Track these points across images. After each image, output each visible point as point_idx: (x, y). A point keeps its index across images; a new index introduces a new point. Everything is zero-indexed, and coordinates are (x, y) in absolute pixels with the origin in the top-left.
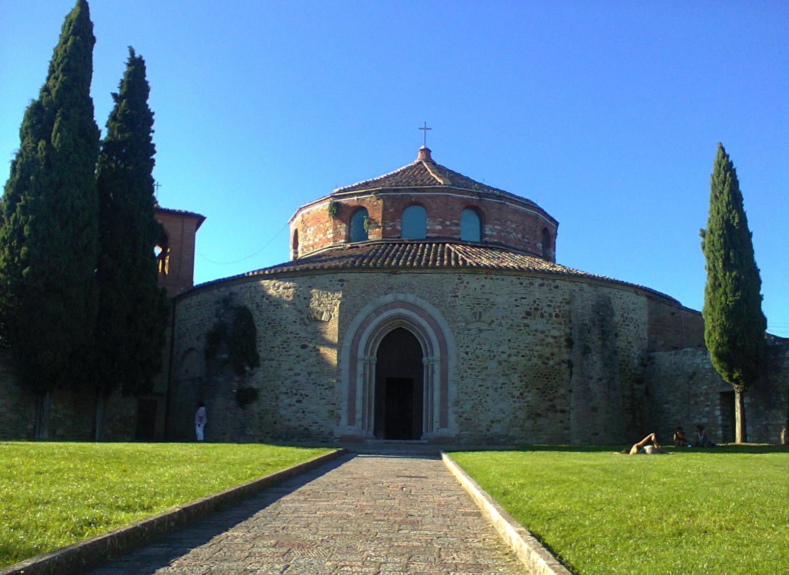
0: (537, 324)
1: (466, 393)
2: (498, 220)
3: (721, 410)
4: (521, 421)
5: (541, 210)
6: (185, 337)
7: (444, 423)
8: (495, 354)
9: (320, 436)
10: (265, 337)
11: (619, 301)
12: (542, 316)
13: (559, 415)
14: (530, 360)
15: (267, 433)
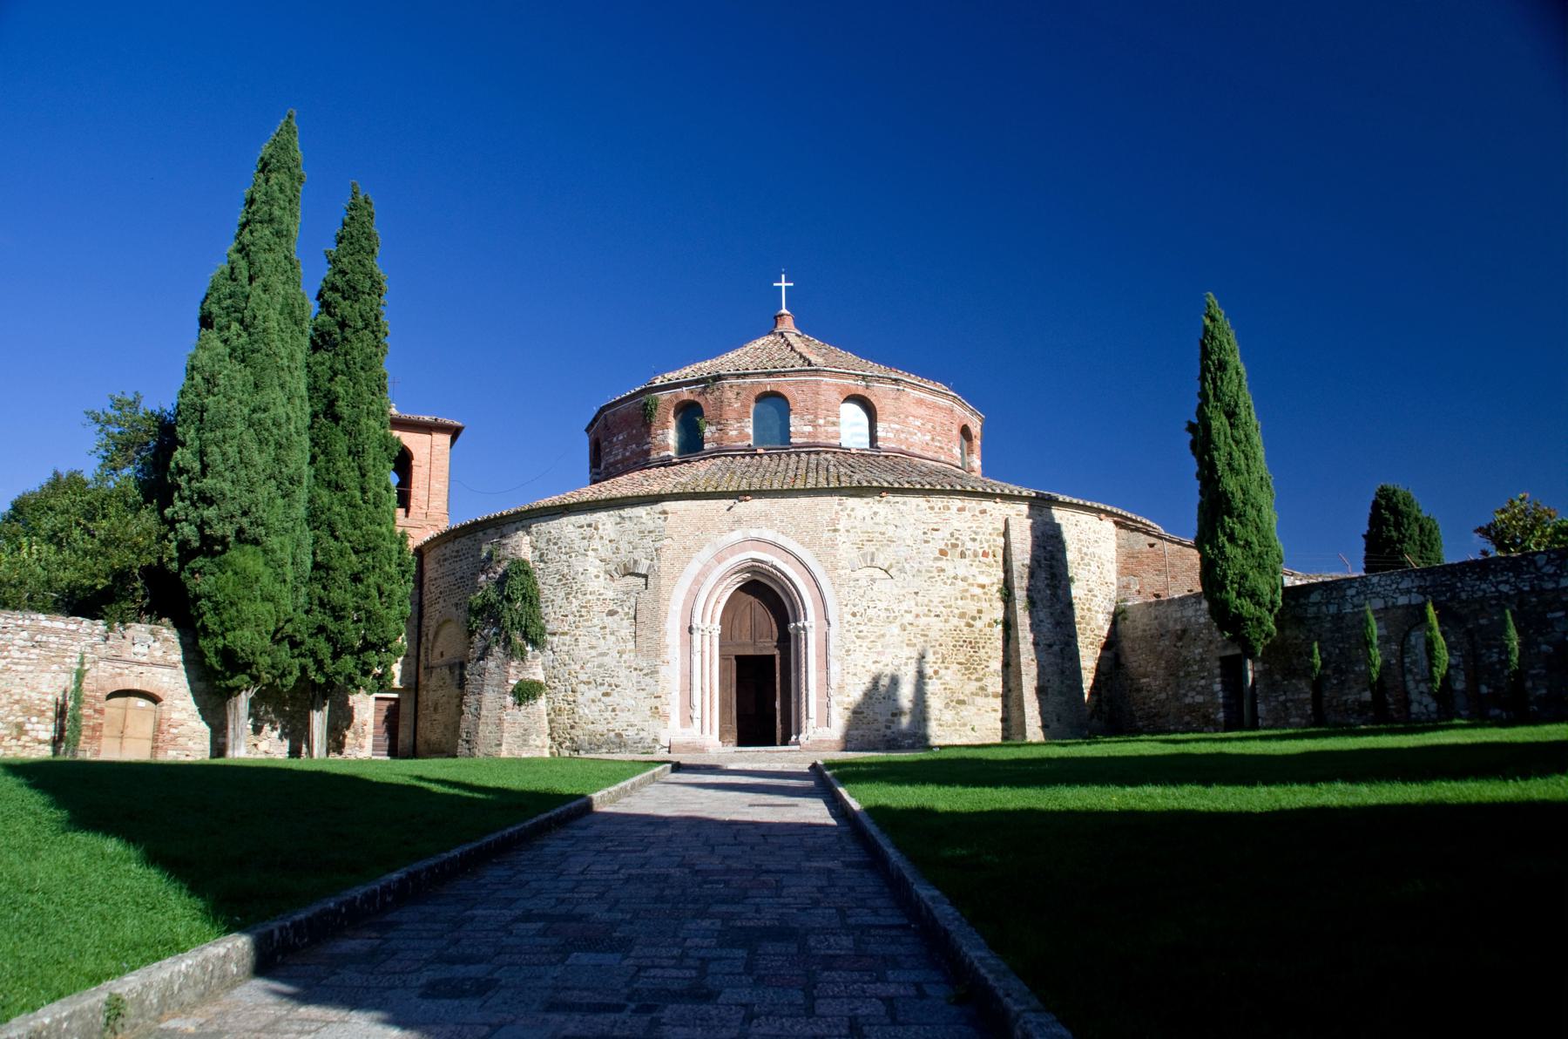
1: (855, 674)
2: (895, 415)
3: (1223, 682)
8: (897, 614)
9: (640, 745)
10: (553, 600)
12: (963, 555)
14: (946, 621)
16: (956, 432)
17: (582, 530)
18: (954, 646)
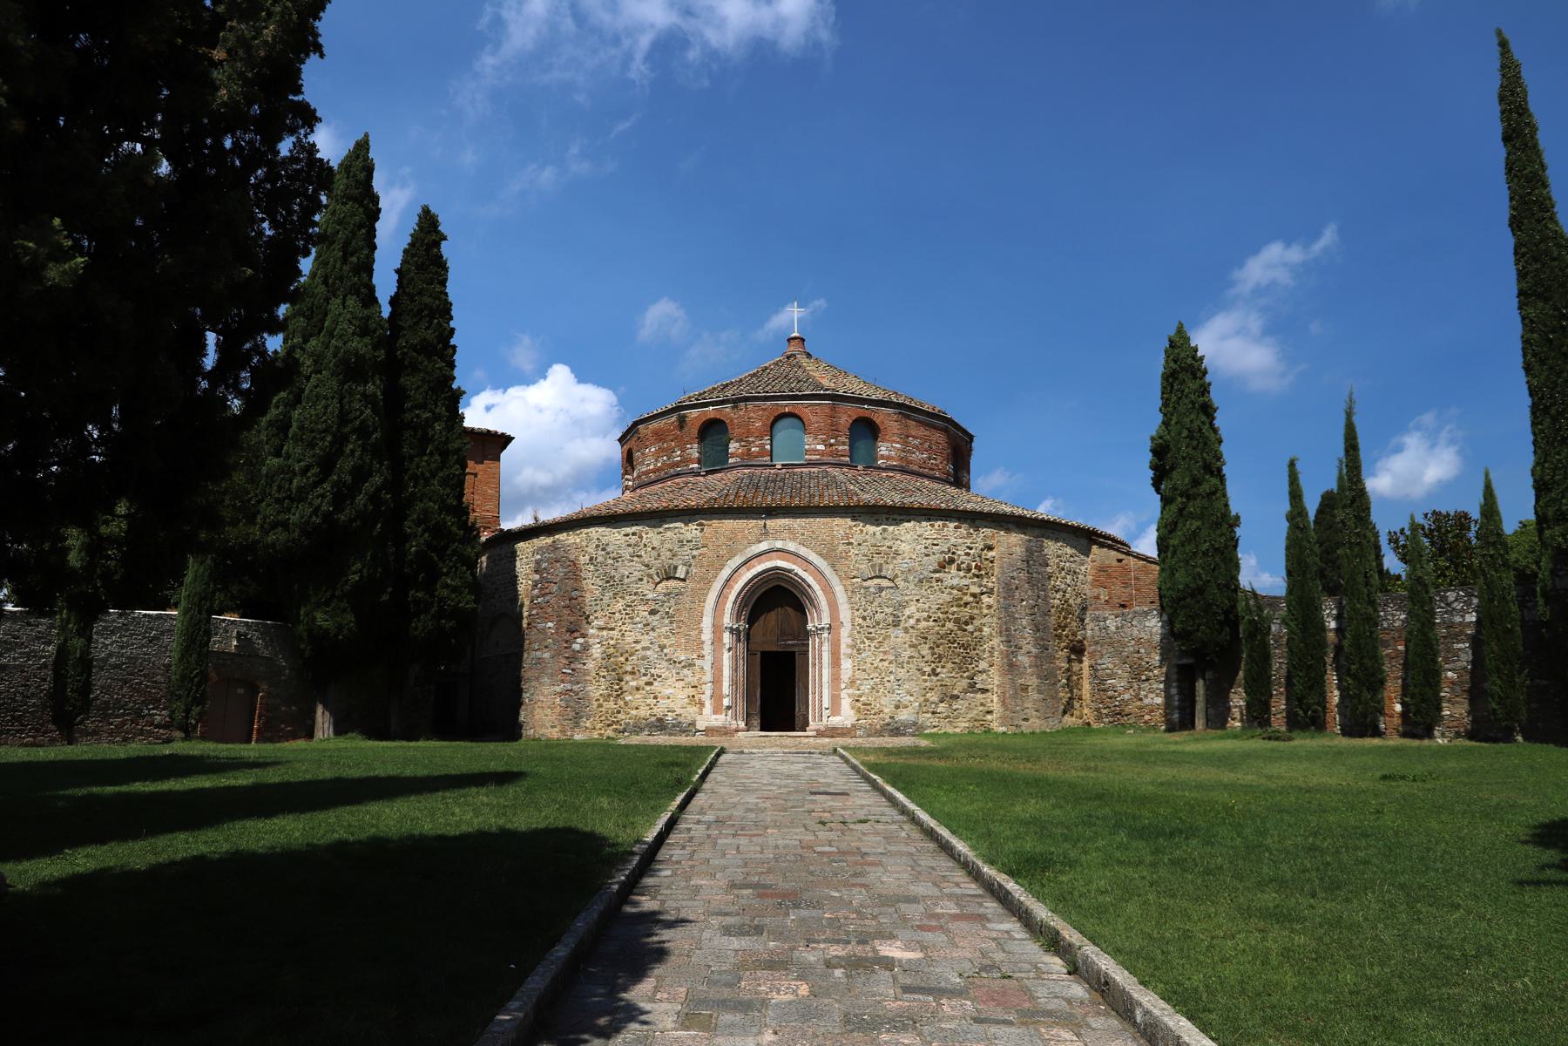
0: (953, 577)
1: (864, 670)
7: (835, 708)
13: (979, 696)
15: (609, 725)
18: (950, 648)
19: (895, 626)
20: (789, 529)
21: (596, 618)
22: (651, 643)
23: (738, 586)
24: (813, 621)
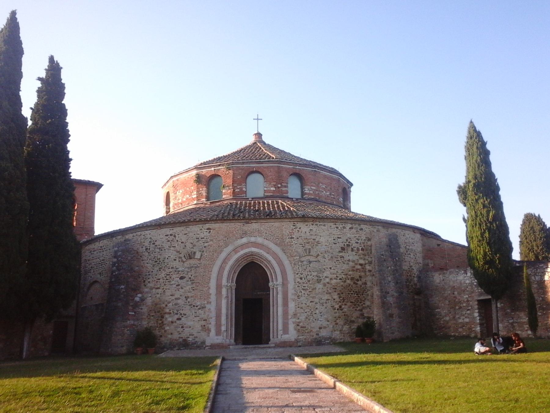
0: (350, 256)
1: (302, 308)
3: (479, 312)
4: (341, 327)
5: (341, 175)
6: (90, 272)
7: (286, 330)
9: (195, 345)
10: (152, 272)
11: (404, 238)
12: (352, 250)
16: (340, 191)
17: (167, 237)
19: (318, 282)
20: (259, 230)
21: (149, 282)
22: (181, 296)
23: (231, 263)
24: (273, 281)
